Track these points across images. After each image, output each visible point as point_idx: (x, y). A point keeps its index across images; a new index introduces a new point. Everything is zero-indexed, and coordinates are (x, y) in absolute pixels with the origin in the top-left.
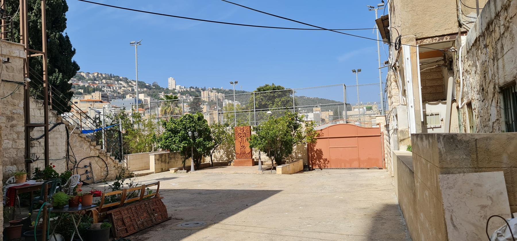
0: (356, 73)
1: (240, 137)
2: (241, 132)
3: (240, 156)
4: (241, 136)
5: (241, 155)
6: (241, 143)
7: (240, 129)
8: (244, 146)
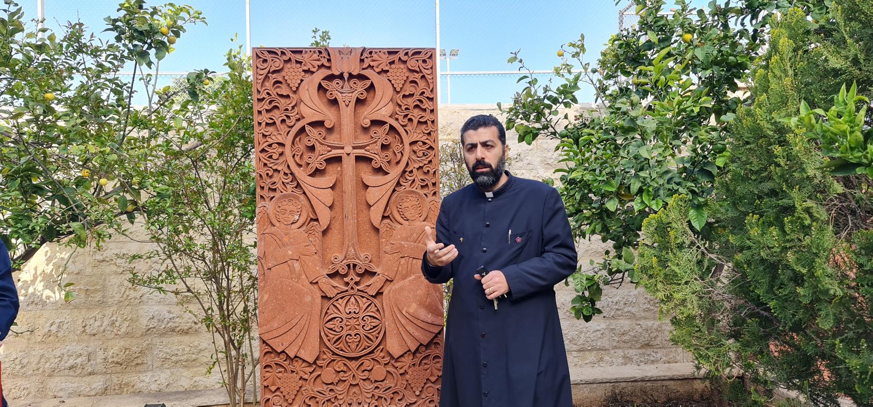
0: (448, 60)
1: (317, 173)
2: (329, 116)
4: (338, 160)
5: (329, 375)
6: (325, 233)
8: (362, 266)
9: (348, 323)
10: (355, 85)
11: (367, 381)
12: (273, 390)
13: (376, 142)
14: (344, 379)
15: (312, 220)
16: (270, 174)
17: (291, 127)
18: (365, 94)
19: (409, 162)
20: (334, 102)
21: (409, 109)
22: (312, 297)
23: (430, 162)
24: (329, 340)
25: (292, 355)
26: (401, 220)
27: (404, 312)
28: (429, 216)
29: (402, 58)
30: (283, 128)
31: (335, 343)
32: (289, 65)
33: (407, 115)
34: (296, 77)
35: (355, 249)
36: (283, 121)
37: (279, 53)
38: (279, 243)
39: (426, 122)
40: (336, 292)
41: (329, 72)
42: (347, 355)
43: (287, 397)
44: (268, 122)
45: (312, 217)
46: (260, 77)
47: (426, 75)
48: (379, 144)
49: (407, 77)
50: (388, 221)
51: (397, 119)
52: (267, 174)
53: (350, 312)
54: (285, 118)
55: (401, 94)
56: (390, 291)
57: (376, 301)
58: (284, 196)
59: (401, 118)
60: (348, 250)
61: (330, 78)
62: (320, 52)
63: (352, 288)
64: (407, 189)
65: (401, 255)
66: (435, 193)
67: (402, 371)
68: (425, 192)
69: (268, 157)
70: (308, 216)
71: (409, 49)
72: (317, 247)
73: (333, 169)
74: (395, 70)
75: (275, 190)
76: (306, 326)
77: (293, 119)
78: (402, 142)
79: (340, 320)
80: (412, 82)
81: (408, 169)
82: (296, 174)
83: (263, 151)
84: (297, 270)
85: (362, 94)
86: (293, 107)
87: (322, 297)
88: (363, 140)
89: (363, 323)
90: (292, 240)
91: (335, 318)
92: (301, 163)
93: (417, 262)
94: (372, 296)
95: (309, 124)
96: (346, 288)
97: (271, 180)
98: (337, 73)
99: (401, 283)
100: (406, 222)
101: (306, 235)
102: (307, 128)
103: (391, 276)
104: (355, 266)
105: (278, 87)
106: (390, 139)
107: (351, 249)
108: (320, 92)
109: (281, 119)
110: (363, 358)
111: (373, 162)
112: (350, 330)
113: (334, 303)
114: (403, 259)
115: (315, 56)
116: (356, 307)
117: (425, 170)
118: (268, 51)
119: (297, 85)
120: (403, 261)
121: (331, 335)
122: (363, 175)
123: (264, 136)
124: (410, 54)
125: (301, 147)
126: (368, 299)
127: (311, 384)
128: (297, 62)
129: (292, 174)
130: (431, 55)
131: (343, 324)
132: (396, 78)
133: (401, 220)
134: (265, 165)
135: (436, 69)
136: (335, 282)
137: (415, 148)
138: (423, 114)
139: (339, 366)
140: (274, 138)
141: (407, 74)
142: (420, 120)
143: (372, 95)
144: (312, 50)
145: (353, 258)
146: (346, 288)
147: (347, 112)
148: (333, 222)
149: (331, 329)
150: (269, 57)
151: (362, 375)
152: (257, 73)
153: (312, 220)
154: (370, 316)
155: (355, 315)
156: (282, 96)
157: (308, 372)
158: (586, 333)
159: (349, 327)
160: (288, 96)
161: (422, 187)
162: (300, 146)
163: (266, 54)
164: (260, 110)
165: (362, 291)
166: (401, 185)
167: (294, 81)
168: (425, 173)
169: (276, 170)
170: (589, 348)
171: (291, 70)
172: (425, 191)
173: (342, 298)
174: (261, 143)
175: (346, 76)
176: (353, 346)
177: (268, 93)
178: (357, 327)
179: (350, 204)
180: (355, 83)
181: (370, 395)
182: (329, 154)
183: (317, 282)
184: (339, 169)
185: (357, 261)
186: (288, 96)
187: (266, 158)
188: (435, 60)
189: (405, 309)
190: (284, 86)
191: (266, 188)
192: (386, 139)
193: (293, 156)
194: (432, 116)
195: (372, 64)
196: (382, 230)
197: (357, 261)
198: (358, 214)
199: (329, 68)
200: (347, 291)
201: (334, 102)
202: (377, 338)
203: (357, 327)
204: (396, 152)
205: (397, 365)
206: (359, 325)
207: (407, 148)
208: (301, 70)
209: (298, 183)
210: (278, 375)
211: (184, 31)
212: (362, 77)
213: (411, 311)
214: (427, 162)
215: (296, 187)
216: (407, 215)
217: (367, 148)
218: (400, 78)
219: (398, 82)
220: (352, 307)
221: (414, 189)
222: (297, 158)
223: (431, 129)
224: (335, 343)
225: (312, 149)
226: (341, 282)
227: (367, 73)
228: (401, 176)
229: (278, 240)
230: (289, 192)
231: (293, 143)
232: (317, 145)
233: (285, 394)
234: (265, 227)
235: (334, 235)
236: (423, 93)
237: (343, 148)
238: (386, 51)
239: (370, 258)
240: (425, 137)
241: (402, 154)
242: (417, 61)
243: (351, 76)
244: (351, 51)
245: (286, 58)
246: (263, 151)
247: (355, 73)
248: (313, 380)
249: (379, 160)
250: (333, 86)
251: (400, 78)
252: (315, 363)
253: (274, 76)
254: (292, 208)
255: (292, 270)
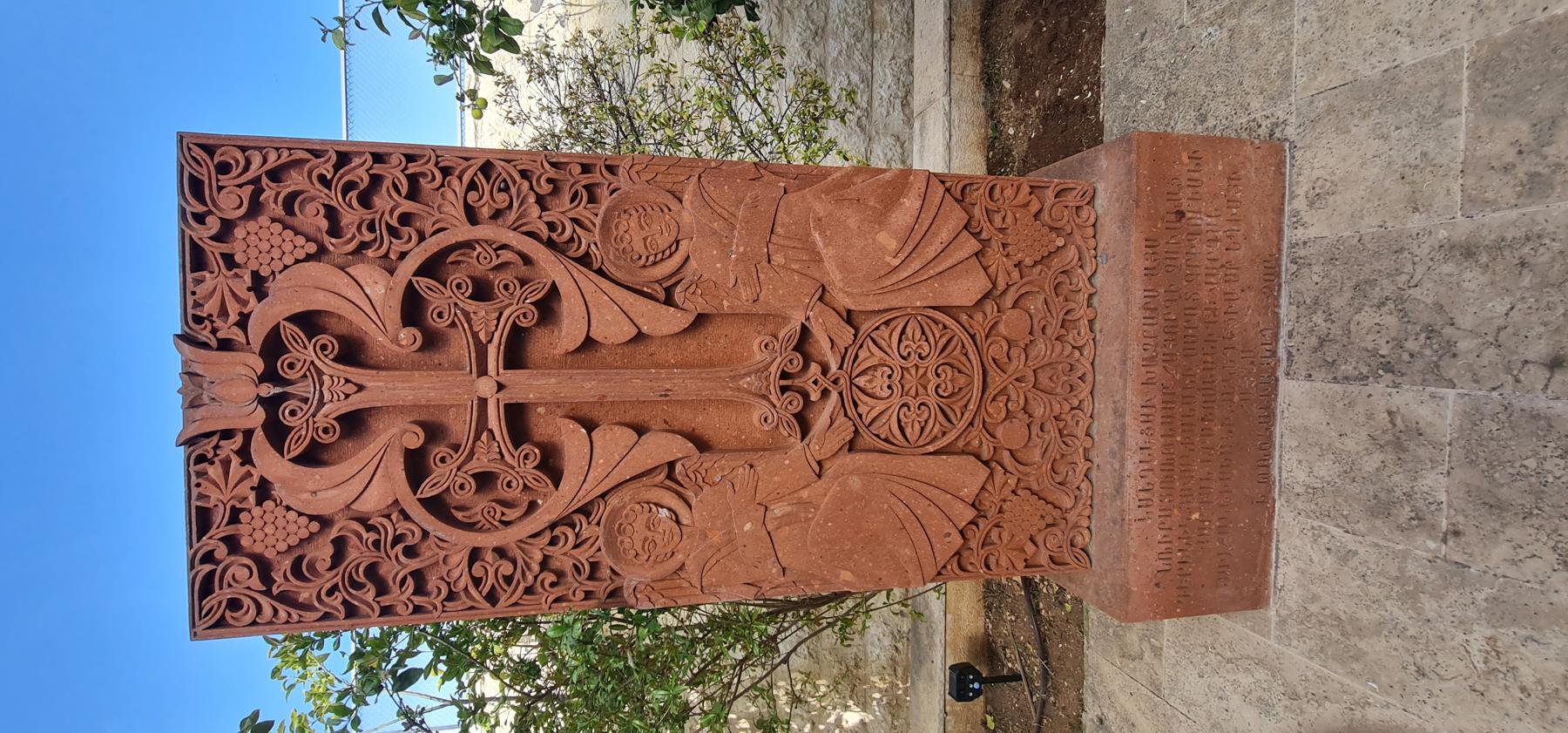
1: (551, 466)
2: (397, 435)
3: (1037, 476)
4: (517, 416)
6: (702, 445)
7: (269, 463)
9: (913, 392)
10: (299, 366)
11: (1028, 351)
12: (1034, 548)
13: (466, 315)
14: (1022, 401)
15: (670, 476)
16: (552, 578)
17: (425, 534)
18: (324, 339)
19: (524, 229)
20: (354, 424)
21: (372, 223)
22: (851, 473)
23: (524, 174)
24: (944, 434)
25: (970, 514)
26: (677, 259)
27: (896, 262)
28: (669, 186)
29: (213, 231)
30: (428, 553)
31: (949, 420)
32: (245, 542)
33: (390, 228)
34: (281, 522)
35: (748, 374)
36: (411, 552)
37: (207, 568)
38: (724, 551)
39: (413, 179)
40: (841, 419)
41: (259, 435)
42: (976, 393)
43: (1049, 520)
44: (411, 590)
45: (663, 476)
46: (283, 615)
47: (268, 166)
48: (471, 306)
49: (274, 220)
50: (678, 289)
51: (403, 255)
52: (553, 585)
53: (889, 387)
54: (399, 548)
55: (329, 241)
56: (848, 294)
57: (865, 327)
58: (611, 543)
59: (398, 246)
60: (749, 392)
61: (277, 433)
62: (201, 459)
63: (835, 382)
64: (597, 239)
65: (765, 263)
66: (611, 169)
67: (1015, 275)
68: (606, 193)
69: (509, 585)
70: (661, 486)
71: (183, 212)
72: (738, 463)
73: (545, 425)
74: (253, 253)
75: (594, 566)
76: (914, 484)
77: (403, 527)
78: (468, 245)
79: (905, 409)
80: (289, 210)
81: (545, 232)
82: (553, 517)
83: (492, 598)
84: (788, 509)
85: (324, 347)
86: (370, 528)
87: (850, 450)
88: (460, 347)
89: (914, 358)
90: (719, 523)
91: (899, 421)
92: (525, 504)
93: (783, 225)
94: (855, 336)
95: (415, 489)
96: (834, 396)
97: (570, 575)
98: (260, 415)
99: (829, 265)
100: (684, 245)
101: (706, 488)
102: (427, 491)
103: (811, 287)
104: (784, 375)
105: (312, 567)
106: (457, 276)
107: (744, 383)
108: (325, 457)
109: (402, 558)
110: (985, 359)
111: (524, 323)
112: (925, 388)
113: (867, 423)
114: (773, 258)
115: (214, 471)
116: (878, 374)
117: (545, 188)
118: (201, 599)
119: (303, 520)
120: (778, 259)
121: (935, 430)
122: (559, 351)
123: (451, 596)
124: (200, 209)
125: (481, 506)
126: (861, 346)
127: (1027, 469)
128: (234, 518)
129: (553, 526)
130: (202, 147)
131: (914, 404)
132: (276, 253)
133: (677, 259)
134: (529, 591)
135: (246, 138)
136: (820, 421)
137: (485, 212)
138: (387, 183)
139: (996, 410)
140: (456, 574)
141: (263, 220)
142: (404, 191)
143: (334, 320)
144: (194, 479)
145: (767, 378)
146: (834, 396)
147: (378, 388)
148: (676, 425)
149: (922, 429)
150: (221, 595)
151: (1017, 364)
152: (270, 623)
153: (670, 476)
154: (900, 341)
155: (897, 377)
156: (338, 558)
157: (1004, 479)
158: (848, 15)
159: (921, 390)
160: (340, 544)
161: (592, 199)
162: (478, 509)
163: (210, 602)
164: (378, 611)
165: (843, 359)
166: (587, 254)
167: (292, 528)
168: (556, 191)
169: (544, 564)
170: (869, 12)
171: (258, 535)
172: (603, 192)
173: (856, 405)
174: (471, 603)
175: (268, 390)
176: (962, 380)
177: (330, 593)
178: (921, 371)
179: (634, 385)
180: (291, 366)
181: (1058, 345)
182: (498, 438)
183: (819, 463)
184: (541, 410)
185: (773, 369)
186: (340, 544)
187: (510, 590)
188: (218, 137)
189: (888, 259)
190: (311, 553)
191: (590, 586)
192: (459, 286)
193: (507, 524)
194: (394, 160)
195: (233, 317)
196: (700, 305)
197: (773, 369)
198: (657, 366)
199: (248, 434)
200: (841, 394)
201: (354, 424)
202: (945, 327)
203: (921, 371)
204: (495, 262)
205: (1001, 285)
206: (917, 367)
207: (484, 231)
208: (257, 511)
209: (581, 510)
210: (1005, 541)
211: (256, 714)
212: (273, 347)
213: (893, 245)
214: (526, 184)
215: (588, 515)
216: (664, 242)
217: (482, 336)
218: (276, 241)
219: (288, 247)
220: (877, 383)
221: (598, 221)
222: (512, 514)
223: (431, 165)
224: (949, 420)
225: (485, 480)
226: (816, 408)
227: (257, 332)
228: (563, 253)
229: (717, 556)
230: (600, 531)
231: (470, 526)
232: (475, 466)
233: (1042, 524)
234: (686, 584)
235: (710, 422)
236: (322, 178)
237: (483, 402)
238: (190, 276)
239: (767, 339)
240: (456, 183)
241: (504, 247)
242: (220, 188)
243: (270, 376)
244: (189, 374)
245: (221, 551)
246: (492, 598)
247: (260, 366)
248: (1021, 467)
249: (517, 307)
250: (302, 426)
251: (276, 241)
252: (986, 463)
253: (278, 577)
254: (639, 524)
255: (788, 519)
